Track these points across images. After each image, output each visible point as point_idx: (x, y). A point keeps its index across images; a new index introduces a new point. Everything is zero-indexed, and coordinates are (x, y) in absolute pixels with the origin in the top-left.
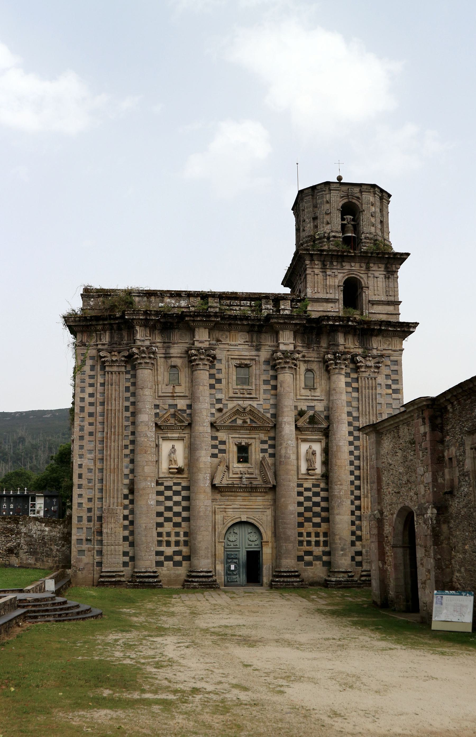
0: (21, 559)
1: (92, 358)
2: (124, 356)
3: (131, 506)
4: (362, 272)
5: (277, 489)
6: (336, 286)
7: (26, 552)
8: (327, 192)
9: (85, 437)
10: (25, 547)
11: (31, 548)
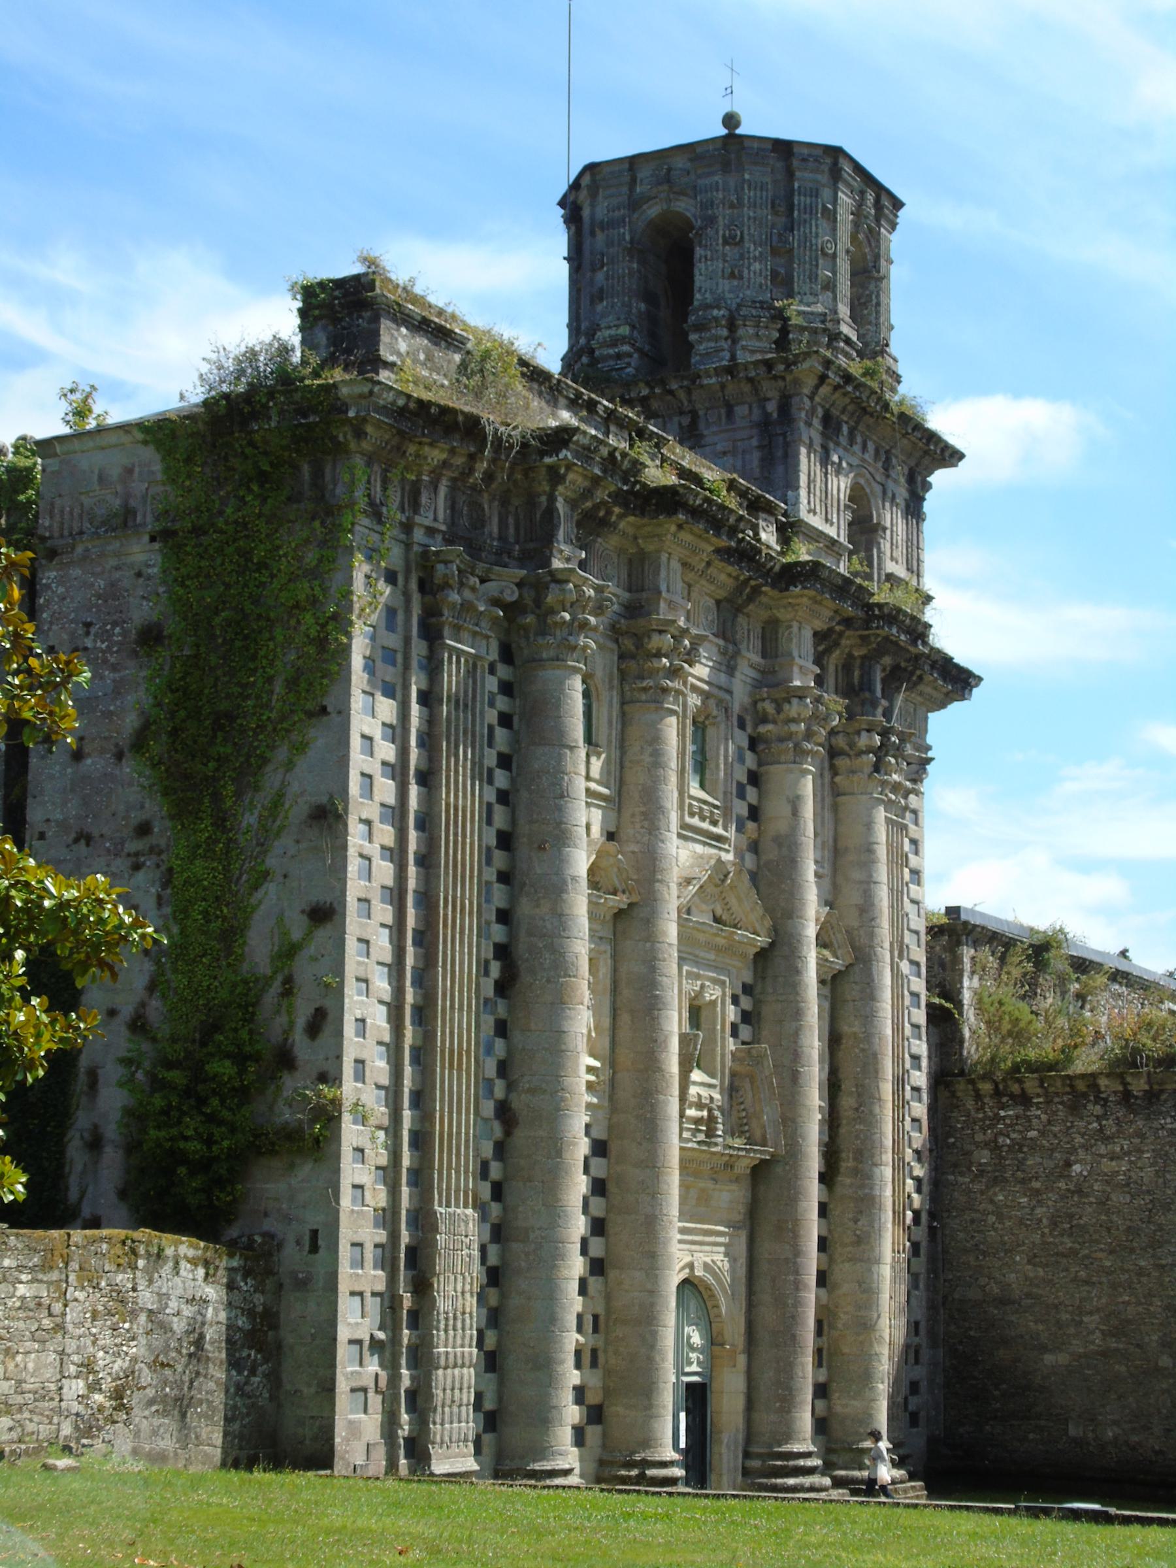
0: (137, 1434)
1: (391, 578)
2: (496, 602)
3: (495, 1209)
4: (878, 478)
5: (779, 1170)
6: (842, 508)
7: (151, 1402)
8: (824, 178)
9: (373, 902)
10: (146, 1376)
11: (165, 1383)
